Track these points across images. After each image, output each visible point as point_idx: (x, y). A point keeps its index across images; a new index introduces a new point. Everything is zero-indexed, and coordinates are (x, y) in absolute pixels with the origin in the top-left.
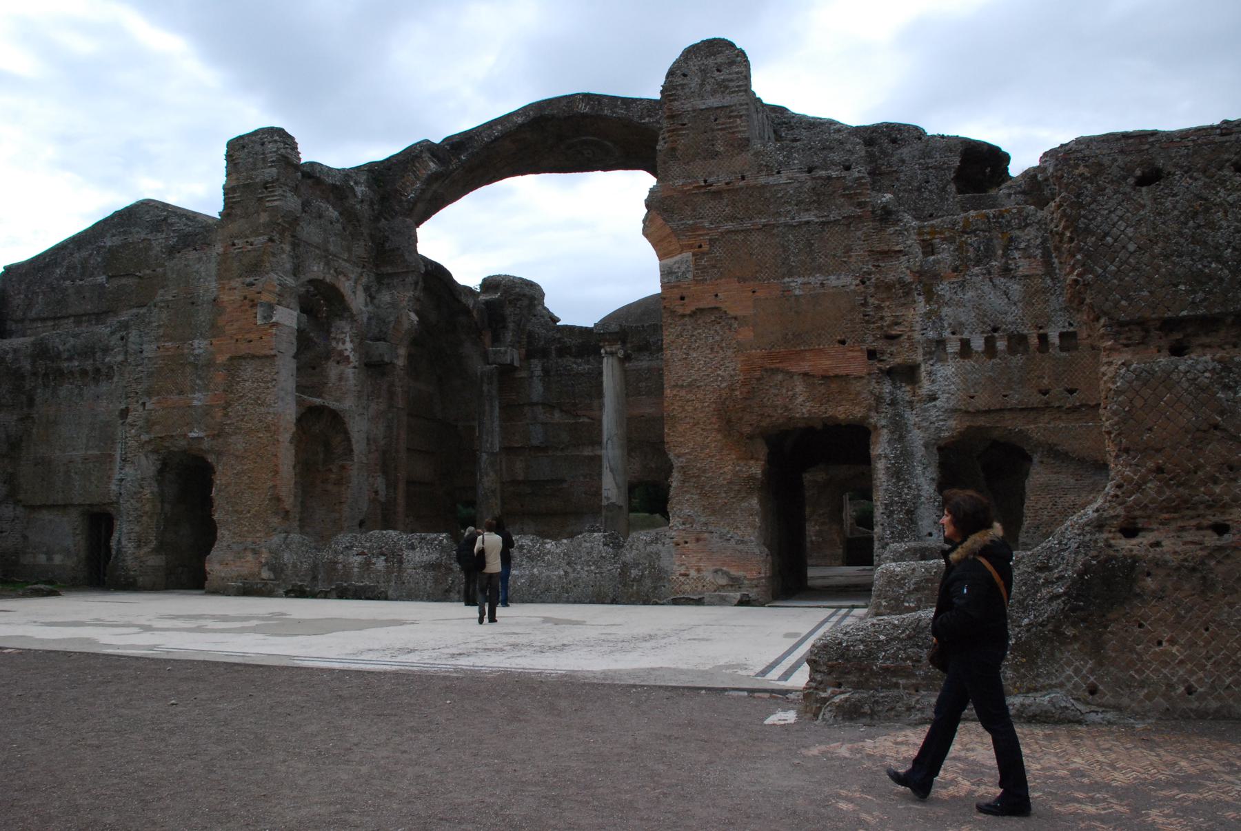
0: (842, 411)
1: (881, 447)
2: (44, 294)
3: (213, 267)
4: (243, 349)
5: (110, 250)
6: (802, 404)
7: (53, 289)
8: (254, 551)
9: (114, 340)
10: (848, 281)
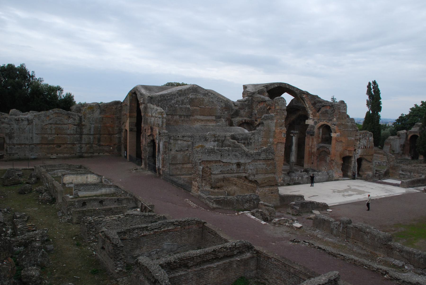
0: (351, 155)
1: (353, 159)
2: (168, 107)
4: (280, 141)
5: (191, 98)
6: (347, 154)
7: (172, 107)
9: (252, 137)
10: (353, 139)
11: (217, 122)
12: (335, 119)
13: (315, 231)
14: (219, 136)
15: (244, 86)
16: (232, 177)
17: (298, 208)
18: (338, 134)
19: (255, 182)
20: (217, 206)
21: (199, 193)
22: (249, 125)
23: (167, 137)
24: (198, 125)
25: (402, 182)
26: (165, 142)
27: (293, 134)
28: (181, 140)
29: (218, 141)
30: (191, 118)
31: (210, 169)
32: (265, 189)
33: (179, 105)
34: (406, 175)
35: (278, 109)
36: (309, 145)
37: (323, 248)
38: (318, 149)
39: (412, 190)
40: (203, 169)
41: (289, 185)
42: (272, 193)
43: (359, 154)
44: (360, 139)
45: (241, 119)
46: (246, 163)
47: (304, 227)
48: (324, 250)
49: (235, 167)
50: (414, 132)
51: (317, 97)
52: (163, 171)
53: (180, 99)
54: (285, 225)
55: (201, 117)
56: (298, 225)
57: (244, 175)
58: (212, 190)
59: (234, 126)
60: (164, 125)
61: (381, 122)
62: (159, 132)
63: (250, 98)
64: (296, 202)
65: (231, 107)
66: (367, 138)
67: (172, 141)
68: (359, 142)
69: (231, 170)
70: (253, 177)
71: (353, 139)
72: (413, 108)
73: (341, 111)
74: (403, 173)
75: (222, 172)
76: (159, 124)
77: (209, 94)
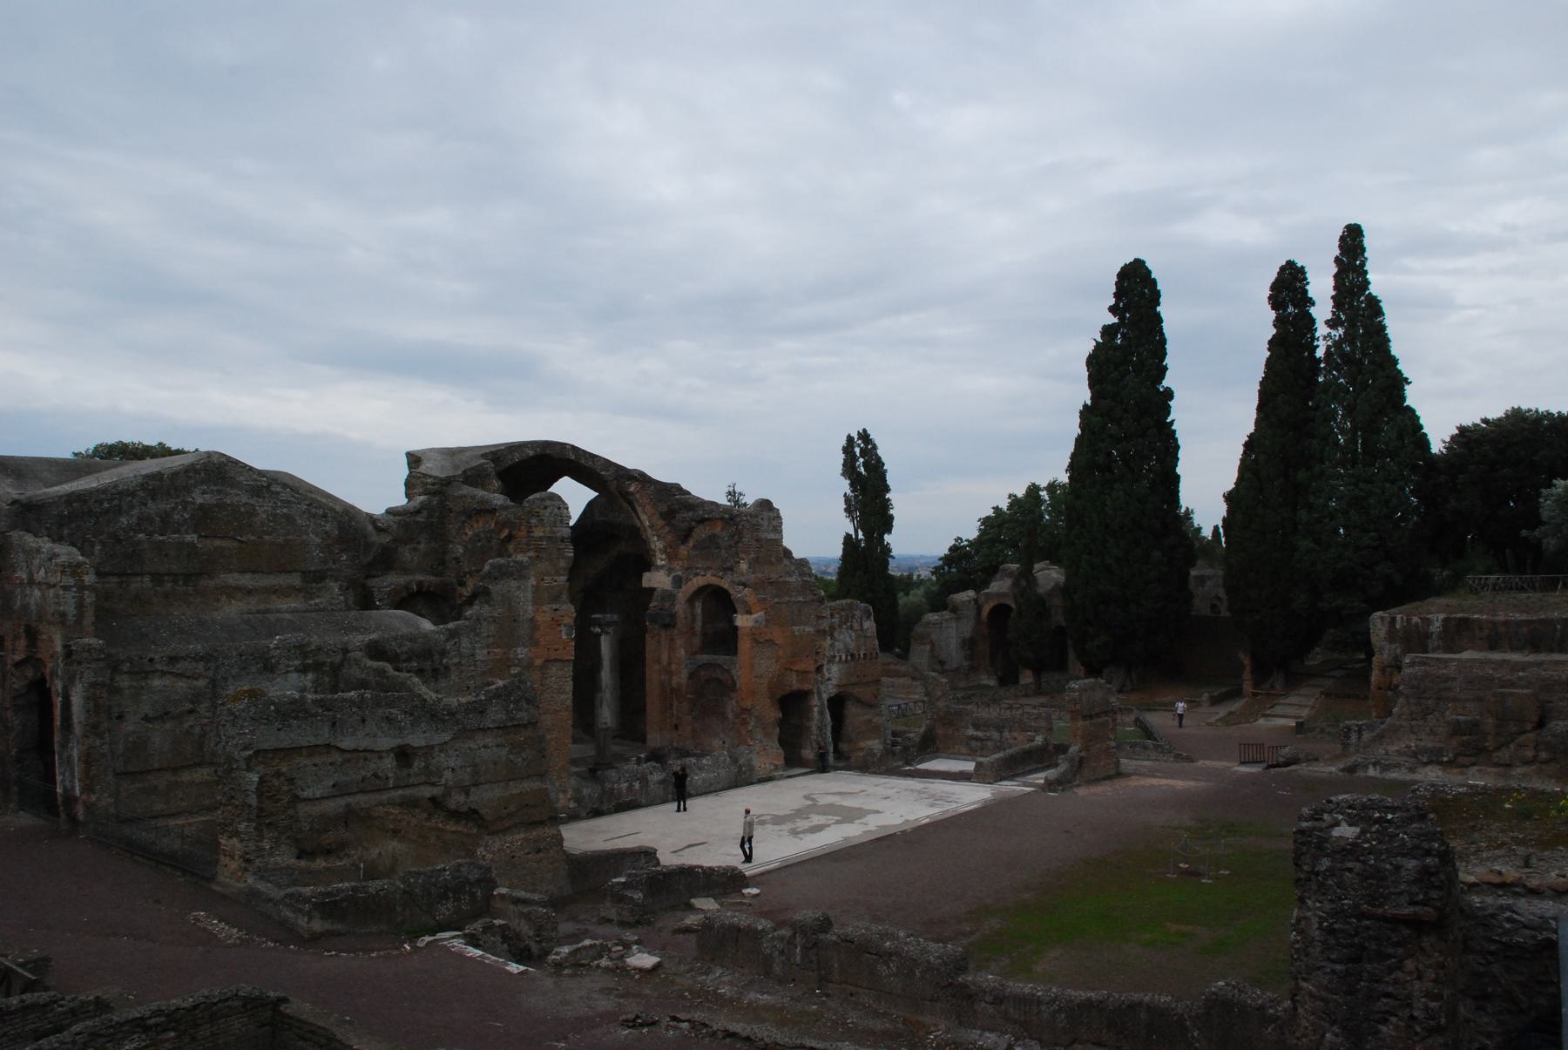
0: (806, 687)
1: (815, 701)
2: (103, 544)
3: (529, 595)
4: (553, 655)
5: (201, 507)
6: (794, 683)
7: (119, 541)
8: (565, 792)
10: (809, 629)
11: (310, 595)
12: (744, 566)
13: (707, 974)
14: (319, 649)
15: (409, 455)
16: (381, 804)
17: (638, 896)
18: (759, 615)
19: (472, 815)
20: (328, 926)
21: (250, 881)
22: (435, 600)
23: (101, 664)
24: (231, 610)
25: (979, 765)
26: (93, 685)
27: (600, 625)
28: (164, 673)
29: (317, 667)
30: (204, 582)
31: (291, 781)
32: (509, 838)
33: (150, 534)
34: (989, 739)
35: (541, 538)
36: (659, 661)
37: (744, 1034)
38: (692, 676)
39: (1010, 787)
40: (262, 781)
41: (597, 813)
42: (539, 851)
43: (834, 682)
44: (832, 628)
45: (402, 580)
46: (432, 747)
47: (666, 965)
48: (748, 1039)
49: (389, 763)
50: (999, 595)
51: (677, 488)
52: (89, 807)
53: (153, 508)
54: (598, 966)
55: (246, 580)
56: (645, 960)
57: (427, 792)
58: (303, 863)
59: (378, 608)
60: (89, 618)
61: (894, 569)
62: (66, 647)
63: (435, 500)
64: (629, 875)
65: (365, 537)
66: (856, 626)
67: (124, 682)
68: (829, 641)
69: (376, 776)
70: (462, 798)
71: (809, 629)
72: (988, 518)
73: (763, 535)
74: (980, 734)
75: (340, 790)
76: (63, 615)
77: (273, 488)
